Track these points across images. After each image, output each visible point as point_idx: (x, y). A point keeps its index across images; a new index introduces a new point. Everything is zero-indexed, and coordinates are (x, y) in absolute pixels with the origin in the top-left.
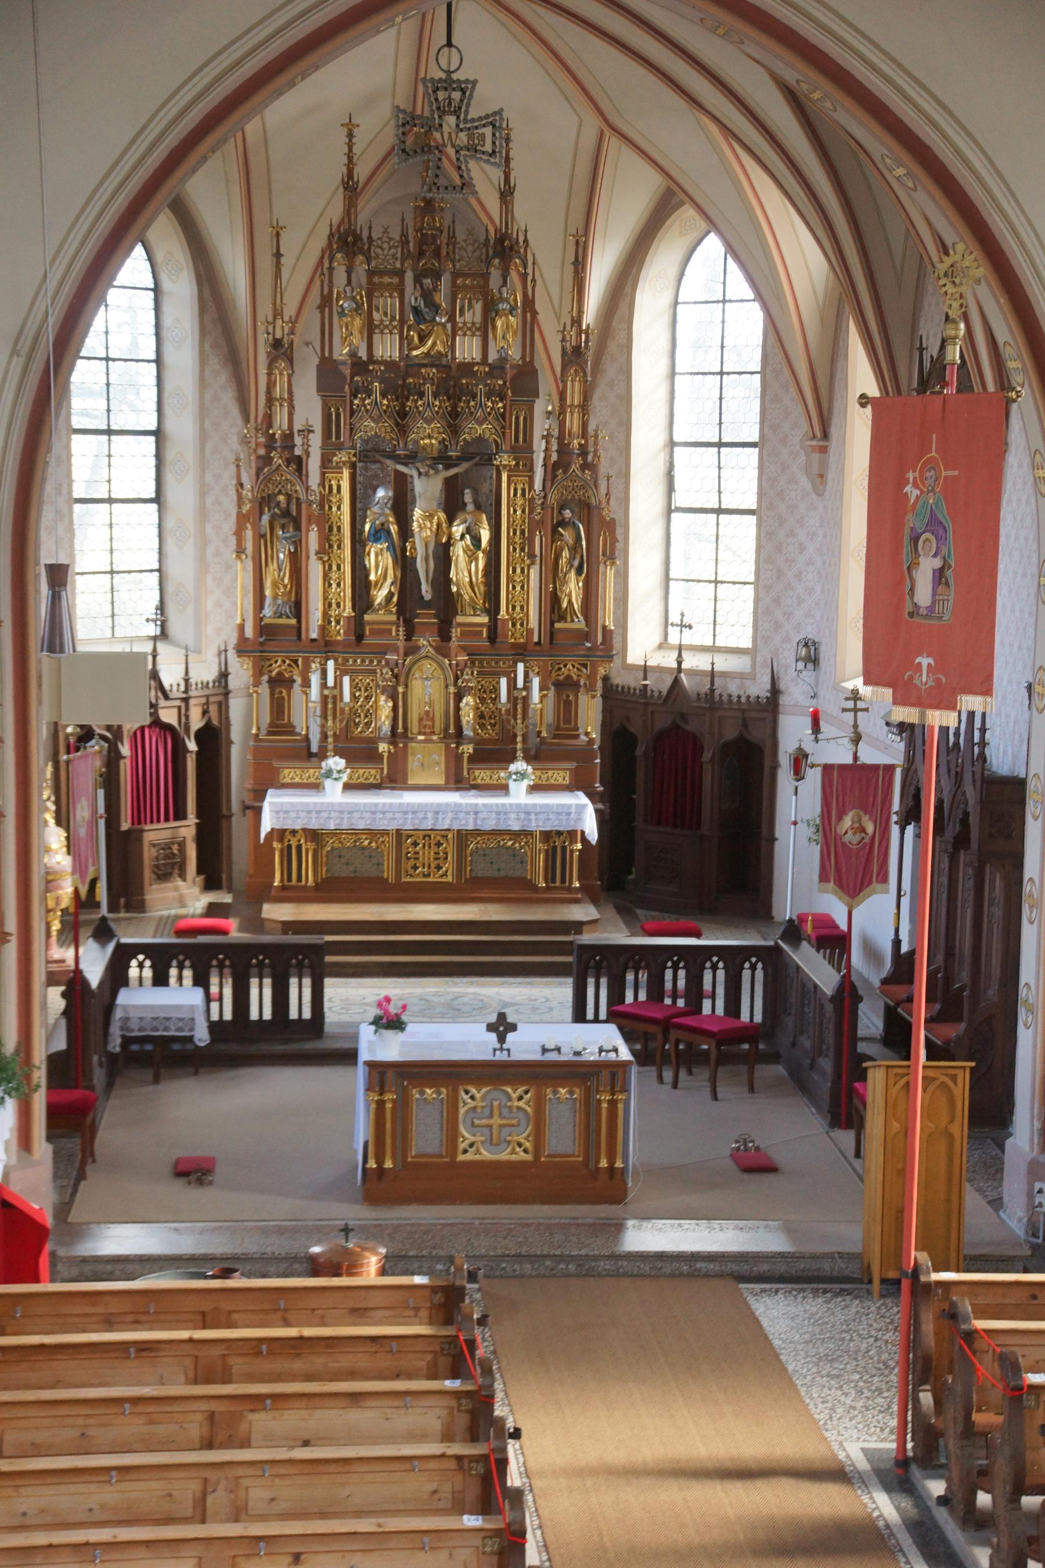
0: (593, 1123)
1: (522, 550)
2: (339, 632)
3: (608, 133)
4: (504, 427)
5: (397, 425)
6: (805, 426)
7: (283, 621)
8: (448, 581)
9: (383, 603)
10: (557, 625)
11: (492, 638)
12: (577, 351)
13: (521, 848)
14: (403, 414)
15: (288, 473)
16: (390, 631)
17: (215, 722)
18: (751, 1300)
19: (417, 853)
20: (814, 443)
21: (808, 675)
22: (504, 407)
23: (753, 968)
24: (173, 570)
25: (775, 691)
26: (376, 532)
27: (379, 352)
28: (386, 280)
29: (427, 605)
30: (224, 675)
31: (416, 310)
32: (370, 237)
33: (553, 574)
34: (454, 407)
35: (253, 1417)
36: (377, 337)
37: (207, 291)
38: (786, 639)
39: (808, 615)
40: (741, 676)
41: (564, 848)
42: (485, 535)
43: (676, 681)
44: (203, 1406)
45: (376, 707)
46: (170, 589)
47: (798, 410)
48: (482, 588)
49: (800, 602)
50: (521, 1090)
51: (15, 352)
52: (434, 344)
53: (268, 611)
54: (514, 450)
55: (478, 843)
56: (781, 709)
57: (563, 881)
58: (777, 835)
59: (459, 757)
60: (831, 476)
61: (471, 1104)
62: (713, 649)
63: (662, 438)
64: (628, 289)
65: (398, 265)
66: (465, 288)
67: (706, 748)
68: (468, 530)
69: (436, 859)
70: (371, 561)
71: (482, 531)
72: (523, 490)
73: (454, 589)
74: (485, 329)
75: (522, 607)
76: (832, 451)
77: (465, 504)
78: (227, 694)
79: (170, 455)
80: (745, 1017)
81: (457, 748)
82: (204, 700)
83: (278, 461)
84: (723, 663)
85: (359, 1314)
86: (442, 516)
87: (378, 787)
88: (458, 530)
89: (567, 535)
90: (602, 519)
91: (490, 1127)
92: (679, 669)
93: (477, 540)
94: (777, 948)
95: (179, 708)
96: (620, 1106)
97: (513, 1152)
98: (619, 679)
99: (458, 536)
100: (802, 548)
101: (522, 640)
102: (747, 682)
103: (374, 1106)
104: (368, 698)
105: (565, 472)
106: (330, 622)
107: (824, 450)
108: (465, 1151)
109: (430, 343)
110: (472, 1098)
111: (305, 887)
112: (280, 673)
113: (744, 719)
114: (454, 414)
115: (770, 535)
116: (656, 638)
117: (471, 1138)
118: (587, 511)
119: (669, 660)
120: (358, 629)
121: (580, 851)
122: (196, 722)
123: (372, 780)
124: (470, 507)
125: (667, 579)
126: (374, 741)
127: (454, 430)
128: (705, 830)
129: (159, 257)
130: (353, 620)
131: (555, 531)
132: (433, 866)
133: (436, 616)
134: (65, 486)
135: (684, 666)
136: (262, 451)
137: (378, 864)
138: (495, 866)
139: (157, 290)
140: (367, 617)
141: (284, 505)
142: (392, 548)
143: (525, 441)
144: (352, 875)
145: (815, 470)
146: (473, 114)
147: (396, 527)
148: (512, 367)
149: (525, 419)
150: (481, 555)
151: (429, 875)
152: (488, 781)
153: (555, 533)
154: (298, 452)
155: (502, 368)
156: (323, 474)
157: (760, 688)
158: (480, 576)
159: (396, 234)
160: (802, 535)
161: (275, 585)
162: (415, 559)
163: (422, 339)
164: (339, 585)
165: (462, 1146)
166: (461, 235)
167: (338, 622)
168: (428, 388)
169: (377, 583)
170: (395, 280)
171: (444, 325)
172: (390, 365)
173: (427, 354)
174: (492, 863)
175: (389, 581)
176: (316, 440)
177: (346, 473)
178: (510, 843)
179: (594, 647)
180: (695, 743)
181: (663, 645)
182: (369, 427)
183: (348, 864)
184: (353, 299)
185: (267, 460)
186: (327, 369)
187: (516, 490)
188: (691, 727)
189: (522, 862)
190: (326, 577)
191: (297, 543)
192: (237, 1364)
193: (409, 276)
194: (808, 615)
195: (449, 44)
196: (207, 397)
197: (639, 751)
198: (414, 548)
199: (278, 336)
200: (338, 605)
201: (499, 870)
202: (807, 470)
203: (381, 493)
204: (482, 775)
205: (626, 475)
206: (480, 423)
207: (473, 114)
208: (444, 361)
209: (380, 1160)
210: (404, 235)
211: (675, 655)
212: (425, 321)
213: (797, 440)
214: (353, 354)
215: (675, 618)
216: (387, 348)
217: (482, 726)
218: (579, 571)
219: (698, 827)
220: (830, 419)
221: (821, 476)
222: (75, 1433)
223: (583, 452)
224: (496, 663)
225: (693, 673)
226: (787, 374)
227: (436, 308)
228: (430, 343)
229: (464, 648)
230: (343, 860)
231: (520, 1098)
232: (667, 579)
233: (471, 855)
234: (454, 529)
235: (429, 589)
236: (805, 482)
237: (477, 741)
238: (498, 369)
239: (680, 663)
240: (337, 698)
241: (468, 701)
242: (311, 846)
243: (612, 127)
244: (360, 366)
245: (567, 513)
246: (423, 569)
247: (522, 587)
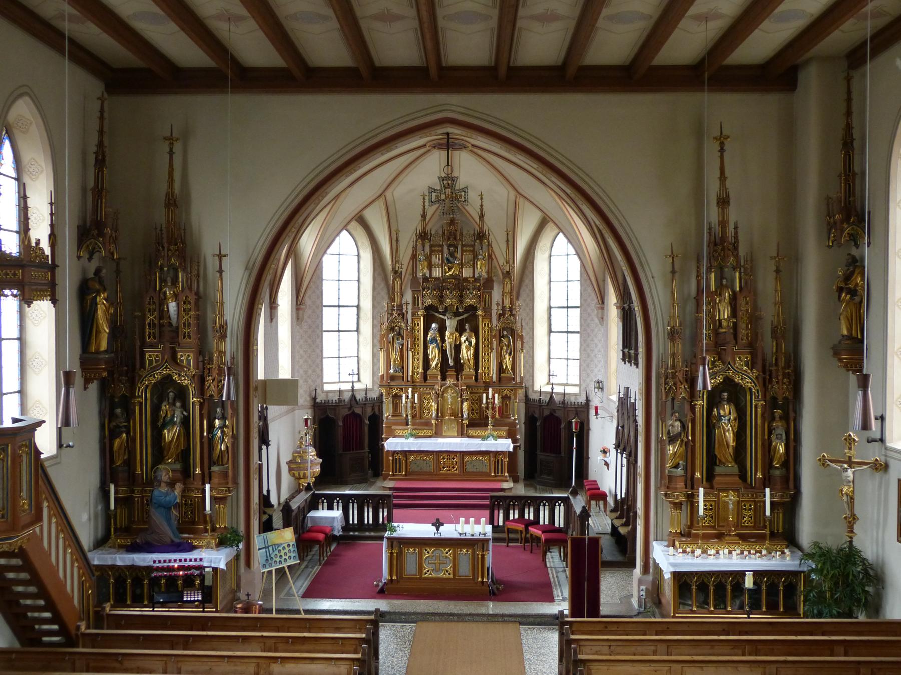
1: (488, 347)
2: (418, 378)
3: (518, 196)
5: (440, 301)
6: (596, 301)
7: (398, 374)
8: (460, 358)
10: (502, 375)
11: (476, 380)
12: (508, 273)
14: (442, 297)
15: (400, 319)
16: (437, 378)
17: (377, 413)
18: (522, 632)
20: (598, 306)
21: (599, 394)
23: (559, 505)
24: (361, 356)
25: (588, 401)
27: (434, 275)
28: (437, 249)
29: (451, 368)
30: (382, 395)
31: (448, 259)
32: (431, 234)
33: (500, 356)
34: (461, 294)
35: (274, 665)
36: (433, 269)
37: (376, 256)
38: (591, 381)
39: (599, 371)
40: (575, 395)
42: (473, 341)
43: (551, 397)
44: (255, 661)
45: (431, 406)
46: (361, 363)
47: (593, 295)
48: (472, 361)
49: (596, 366)
51: (246, 269)
52: (454, 271)
53: (392, 371)
54: (484, 309)
56: (590, 407)
57: (501, 473)
59: (462, 426)
60: (605, 318)
62: (567, 385)
63: (546, 306)
64: (532, 251)
65: (441, 243)
66: (466, 251)
67: (562, 421)
68: (467, 339)
70: (430, 352)
72: (488, 325)
73: (462, 362)
74: (474, 267)
75: (488, 369)
76: (605, 309)
77: (466, 330)
78: (382, 402)
79: (362, 315)
80: (557, 525)
81: (462, 422)
82: (372, 405)
83: (395, 315)
84: (569, 390)
85: (338, 630)
86: (457, 334)
87: (430, 437)
88: (463, 339)
89: (505, 341)
90: (518, 334)
91: (435, 564)
92: (552, 392)
93: (470, 343)
94: (568, 498)
95: (363, 408)
98: (533, 396)
99: (463, 341)
100: (596, 346)
102: (578, 397)
104: (429, 403)
105: (503, 317)
107: (602, 309)
109: (452, 271)
112: (396, 394)
113: (576, 411)
114: (461, 296)
115: (585, 341)
116: (546, 381)
118: (512, 332)
119: (548, 389)
120: (425, 377)
122: (369, 412)
123: (429, 434)
124: (468, 331)
125: (549, 358)
126: (430, 420)
127: (461, 302)
128: (563, 455)
129: (359, 245)
130: (423, 374)
131: (500, 340)
133: (455, 372)
134: (320, 326)
135: (554, 391)
136: (390, 312)
139: (359, 256)
140: (429, 372)
141: (398, 331)
142: (438, 346)
145: (600, 316)
146: (457, 188)
148: (483, 279)
150: (472, 349)
152: (474, 435)
153: (500, 342)
154: (404, 311)
155: (479, 280)
157: (582, 400)
159: (441, 232)
160: (596, 341)
161: (395, 361)
162: (446, 351)
163: (450, 269)
164: (418, 360)
166: (464, 232)
167: (418, 374)
168: (451, 287)
169: (432, 359)
170: (441, 249)
171: (458, 265)
172: (437, 279)
173: (451, 275)
175: (437, 359)
176: (410, 307)
177: (422, 319)
179: (516, 383)
180: (558, 421)
181: (548, 383)
182: (429, 302)
184: (424, 256)
185: (392, 315)
186: (415, 280)
188: (558, 414)
190: (413, 357)
191: (402, 345)
192: (280, 646)
193: (446, 248)
194: (599, 371)
195: (448, 165)
196: (376, 293)
197: (538, 424)
198: (446, 346)
199: (397, 269)
200: (418, 368)
202: (597, 317)
203: (434, 326)
204: (471, 432)
205: (532, 319)
206: (470, 300)
207: (457, 188)
208: (458, 278)
210: (444, 233)
211: (551, 386)
212: (451, 263)
213: (593, 305)
214: (424, 275)
215: (551, 374)
216: (437, 273)
217: (473, 414)
218: (510, 354)
219: (560, 453)
220: (604, 297)
221: (602, 319)
222: (208, 668)
223: (511, 310)
225: (557, 394)
226: (588, 282)
227: (455, 258)
228: (452, 271)
229: (465, 384)
232: (549, 358)
234: (462, 339)
236: (596, 321)
237: (470, 419)
238: (476, 280)
239: (552, 390)
240: (414, 402)
241: (465, 404)
242: (404, 459)
243: (520, 195)
244: (426, 280)
245: (505, 333)
246: (450, 354)
247: (488, 361)
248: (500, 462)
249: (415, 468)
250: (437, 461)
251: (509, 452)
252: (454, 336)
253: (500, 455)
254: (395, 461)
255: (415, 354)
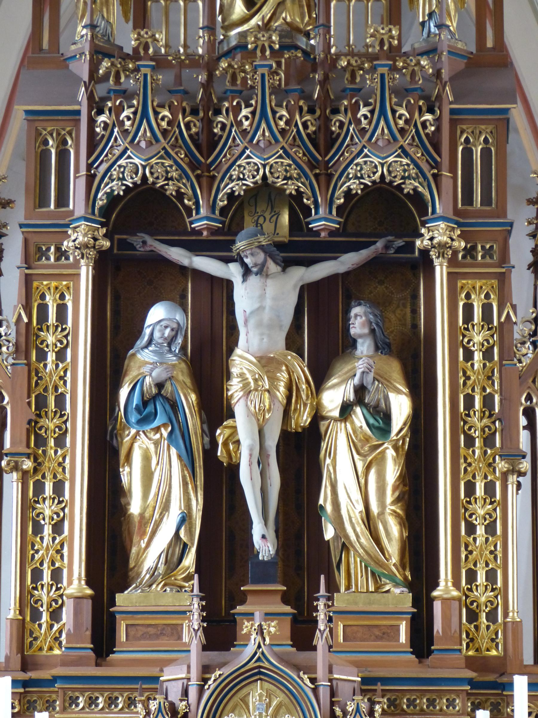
1: (488, 441)
4: (437, 165)
5: (194, 165)
9: (162, 568)
22: (438, 121)
26: (145, 403)
48: (395, 529)
71: (392, 396)
72: (487, 309)
75: (491, 576)
77: (352, 344)
101: (494, 653)
106: (36, 616)
109: (267, 11)
130: (88, 605)
133: (285, 600)
143: (486, 200)
147: (193, 397)
149: (486, 153)
150: (390, 453)
156: (28, 280)
158: (389, 498)
167: (55, 615)
169: (143, 520)
187: (469, 309)
224: (431, 703)
228: (267, 11)
235: (271, 534)
247: (490, 529)
252: (283, 376)
255: (39, 487)
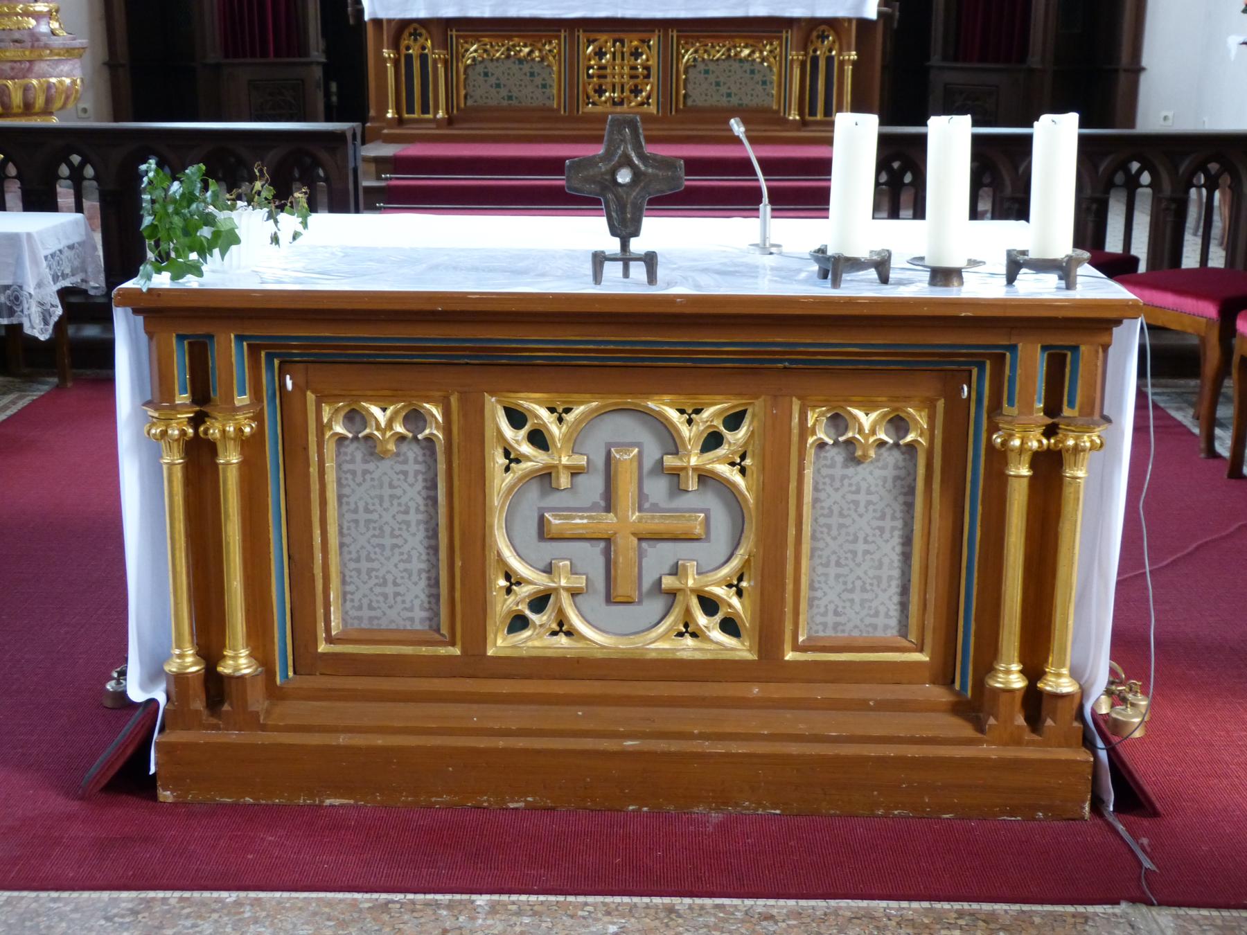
0: (974, 531)
13: (763, 59)
19: (602, 68)
41: (830, 60)
50: (711, 414)
55: (696, 51)
58: (1145, 62)
61: (535, 458)
69: (632, 77)
96: (1078, 473)
97: (689, 629)
103: (173, 459)
108: (518, 623)
110: (538, 439)
111: (435, 120)
117: (536, 580)
121: (854, 63)
128: (1034, 61)
132: (627, 88)
137: (544, 86)
138: (724, 90)
144: (505, 103)
151: (621, 103)
165: (503, 605)
174: (718, 84)
178: (746, 52)
183: (498, 86)
189: (764, 83)
201: (729, 95)
209: (210, 652)
230: (492, 80)
231: (713, 441)
233: (686, 72)
248: (822, 64)
249: (483, 93)
250: (572, 61)
251: (863, 23)
253: (823, 37)
254: (404, 64)
